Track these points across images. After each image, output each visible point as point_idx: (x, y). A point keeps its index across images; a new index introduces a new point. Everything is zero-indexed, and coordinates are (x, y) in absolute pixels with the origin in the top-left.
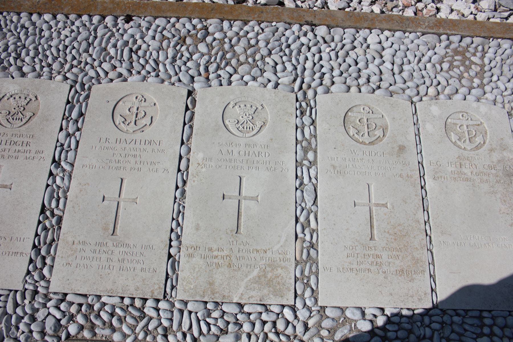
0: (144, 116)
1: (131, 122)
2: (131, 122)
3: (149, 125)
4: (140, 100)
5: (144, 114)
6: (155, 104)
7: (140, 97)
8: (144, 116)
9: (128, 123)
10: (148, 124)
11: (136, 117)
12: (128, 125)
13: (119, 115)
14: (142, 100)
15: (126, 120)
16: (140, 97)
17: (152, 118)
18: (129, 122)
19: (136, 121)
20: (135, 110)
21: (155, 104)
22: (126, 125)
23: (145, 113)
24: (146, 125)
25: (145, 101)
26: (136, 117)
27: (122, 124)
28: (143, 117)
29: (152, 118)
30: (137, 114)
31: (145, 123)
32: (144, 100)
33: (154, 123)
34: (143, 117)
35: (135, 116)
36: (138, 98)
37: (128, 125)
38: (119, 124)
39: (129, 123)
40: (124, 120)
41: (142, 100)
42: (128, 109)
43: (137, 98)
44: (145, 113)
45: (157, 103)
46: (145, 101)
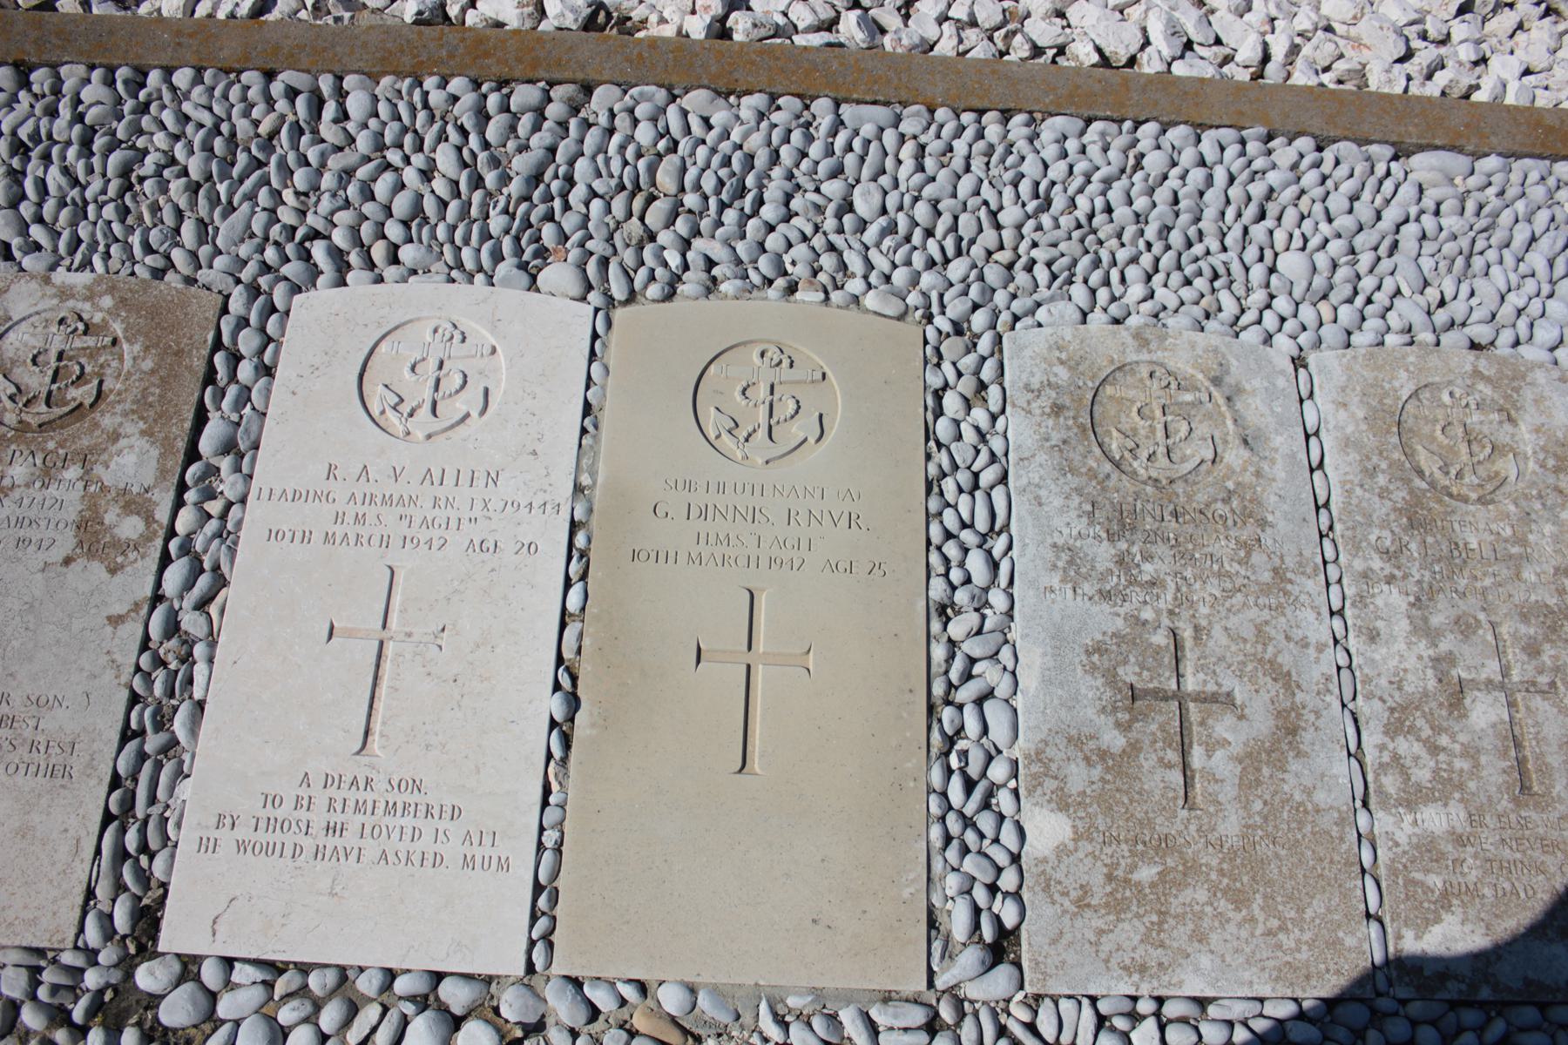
0: (797, 412)
1: (755, 431)
2: (755, 431)
3: (819, 440)
4: (774, 363)
5: (792, 406)
6: (824, 375)
7: (773, 353)
8: (797, 412)
9: (745, 434)
10: (812, 440)
11: (771, 416)
12: (747, 440)
13: (712, 410)
14: (781, 362)
15: (737, 425)
16: (773, 353)
17: (821, 416)
18: (750, 429)
19: (770, 427)
20: (762, 392)
21: (824, 375)
22: (742, 440)
23: (798, 402)
24: (806, 440)
25: (791, 366)
26: (771, 416)
27: (725, 437)
28: (792, 417)
29: (821, 416)
30: (438, 381)
31: (464, 409)
32: (786, 363)
33: (827, 439)
34: (792, 417)
35: (763, 411)
36: (769, 354)
37: (747, 440)
38: (718, 437)
39: (750, 435)
40: (733, 425)
41: (781, 362)
42: (739, 388)
43: (762, 355)
44: (798, 402)
45: (829, 374)
46: (791, 366)
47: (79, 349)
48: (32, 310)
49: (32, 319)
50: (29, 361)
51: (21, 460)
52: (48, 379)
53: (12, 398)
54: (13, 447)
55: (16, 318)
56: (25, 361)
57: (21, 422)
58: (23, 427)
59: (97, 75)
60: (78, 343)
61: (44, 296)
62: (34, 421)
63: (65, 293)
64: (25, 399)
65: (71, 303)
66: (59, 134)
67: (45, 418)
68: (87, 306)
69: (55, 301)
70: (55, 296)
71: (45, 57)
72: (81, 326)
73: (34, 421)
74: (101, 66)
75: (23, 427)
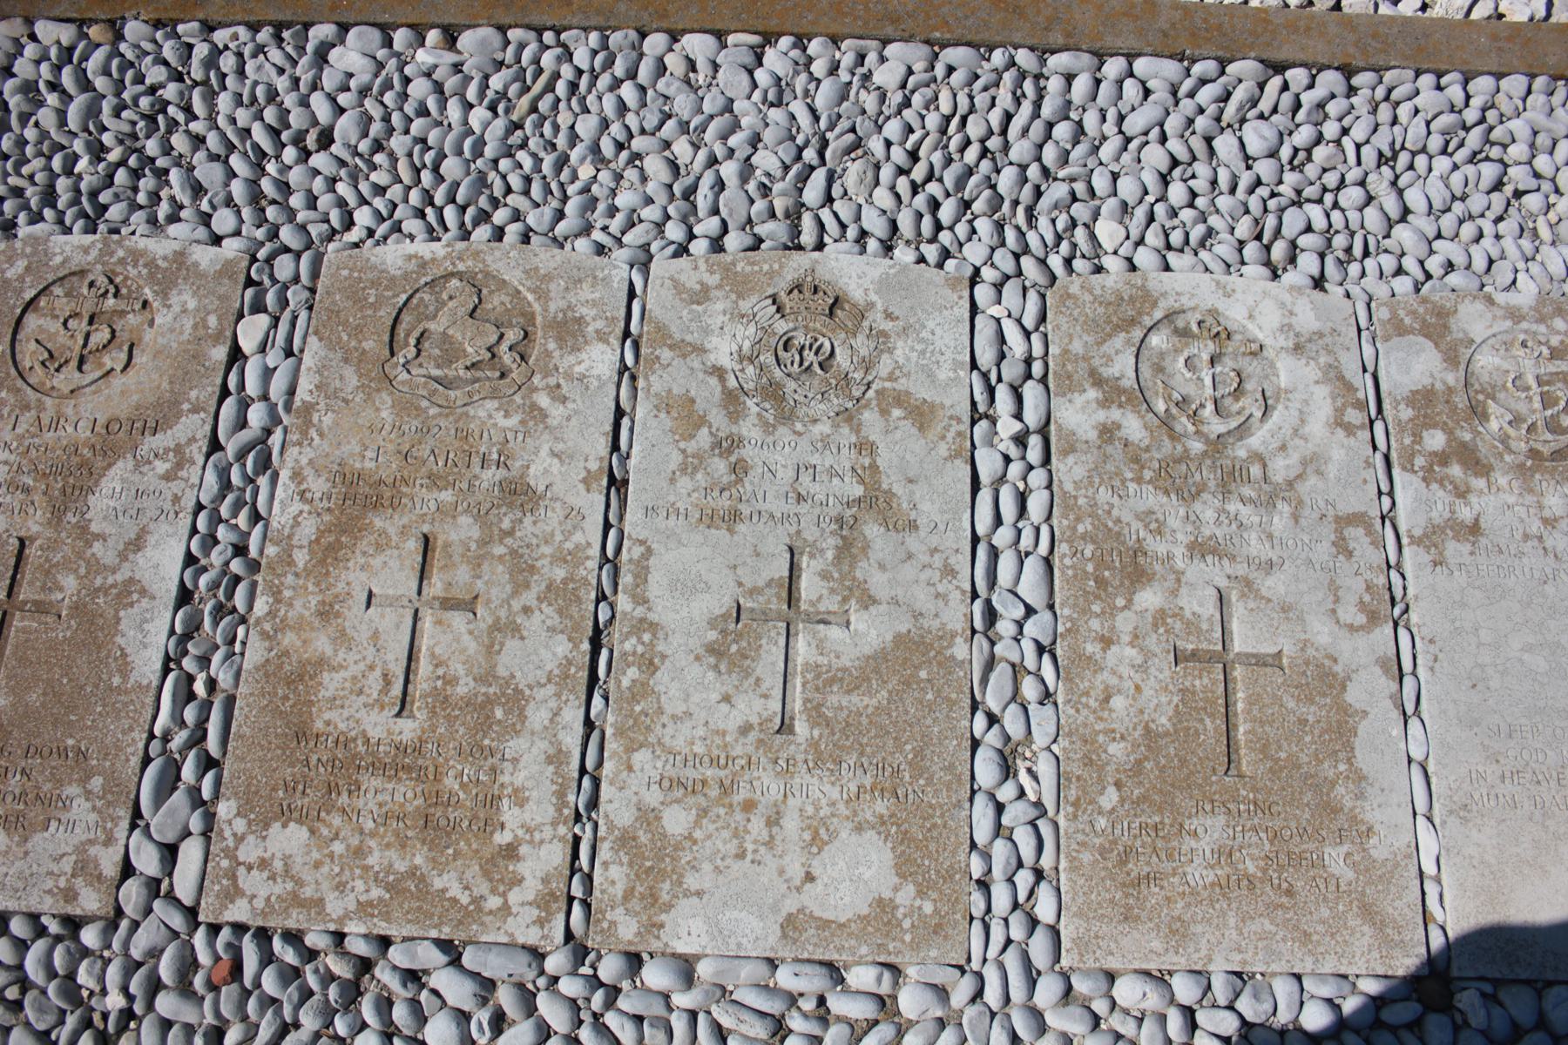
47: (1552, 374)
48: (1490, 332)
49: (1490, 342)
50: (1509, 385)
51: (1551, 490)
52: (1537, 405)
53: (1510, 423)
54: (1538, 476)
55: (1478, 341)
56: (1504, 386)
57: (1531, 450)
58: (1534, 453)
59: (1427, 80)
60: (1552, 368)
61: (1495, 317)
62: (1546, 450)
63: (1515, 315)
64: (1525, 426)
65: (1524, 325)
66: (1414, 144)
67: (1554, 446)
68: (1542, 328)
69: (1508, 323)
70: (1505, 318)
71: (1372, 61)
72: (1546, 351)
73: (1546, 450)
74: (1427, 71)
75: (1534, 453)
